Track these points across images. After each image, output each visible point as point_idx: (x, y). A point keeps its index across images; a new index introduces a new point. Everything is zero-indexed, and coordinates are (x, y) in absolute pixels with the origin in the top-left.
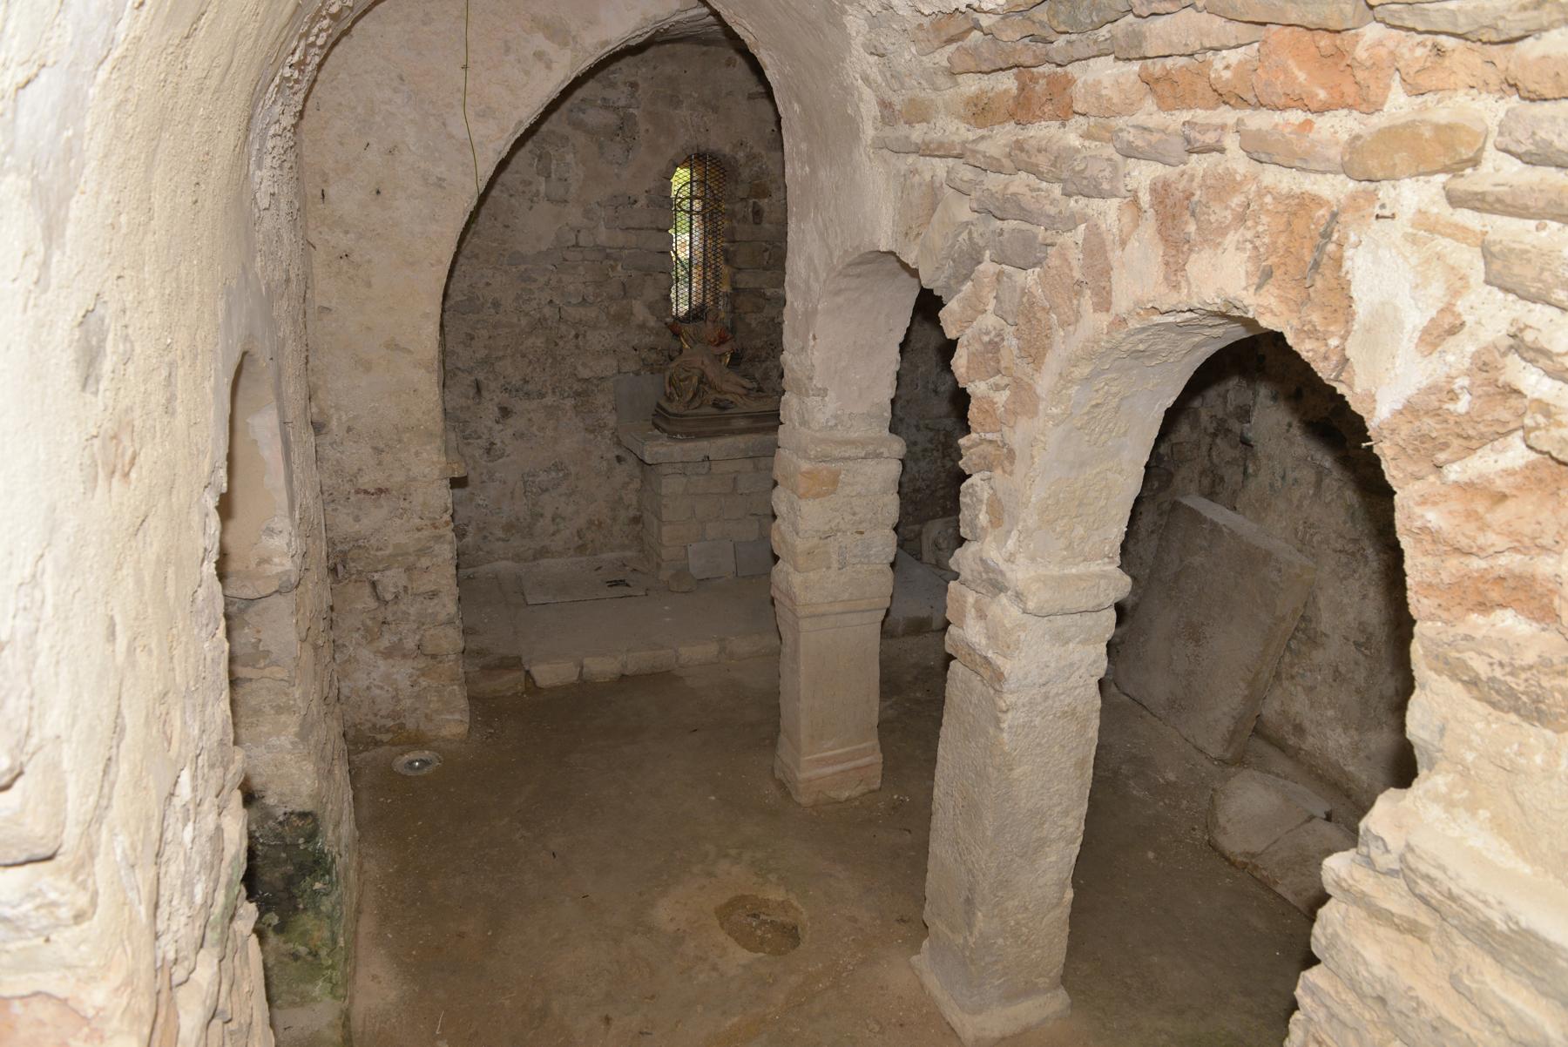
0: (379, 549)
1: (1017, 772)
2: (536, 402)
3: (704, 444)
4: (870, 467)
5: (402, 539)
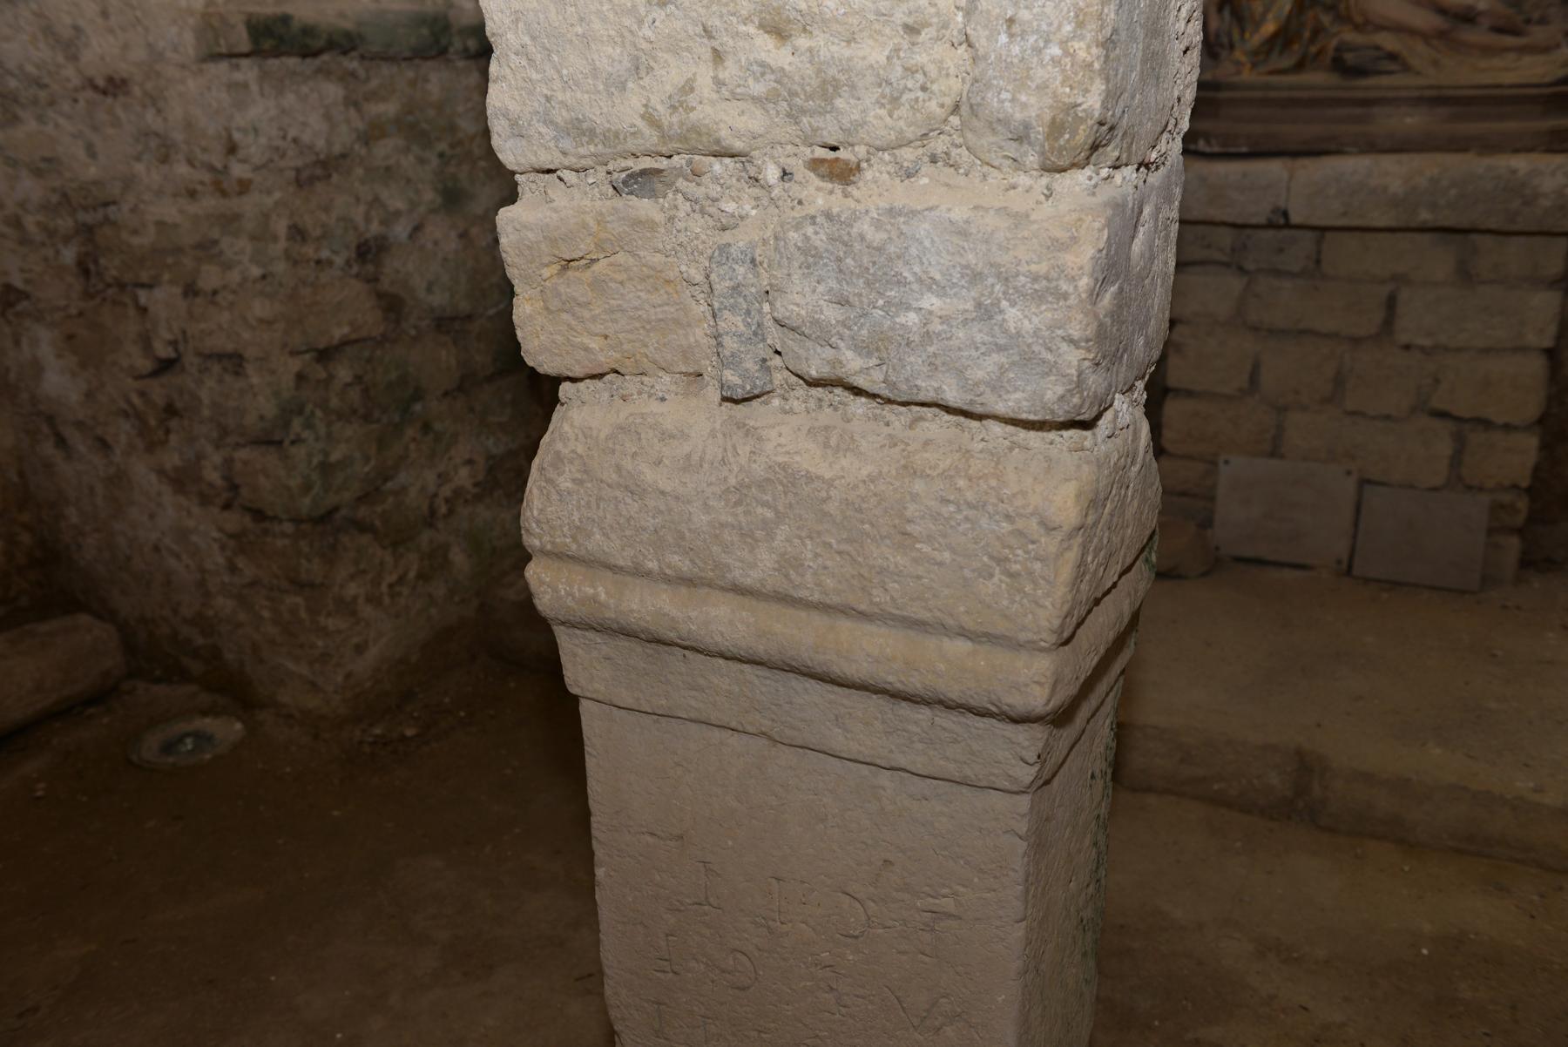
0: (135, 232)
3: (1274, 169)
5: (168, 210)
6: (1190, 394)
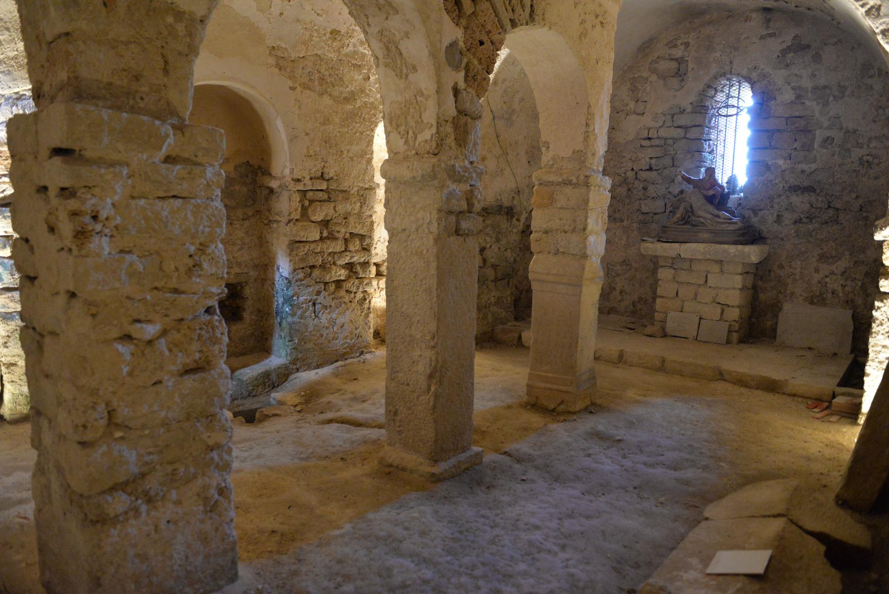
2: (618, 224)
3: (677, 245)
4: (568, 190)
6: (663, 297)
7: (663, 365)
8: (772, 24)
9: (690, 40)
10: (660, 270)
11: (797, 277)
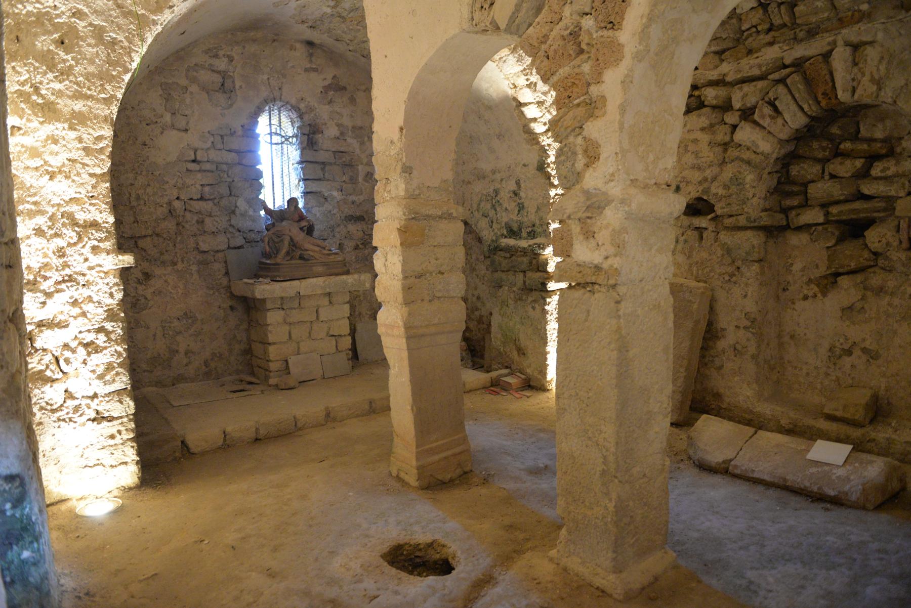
1: (631, 354)
2: (170, 268)
3: (296, 283)
4: (443, 225)
6: (274, 343)
7: (371, 407)
8: (313, 59)
9: (234, 54)
10: (269, 314)
11: (362, 298)
